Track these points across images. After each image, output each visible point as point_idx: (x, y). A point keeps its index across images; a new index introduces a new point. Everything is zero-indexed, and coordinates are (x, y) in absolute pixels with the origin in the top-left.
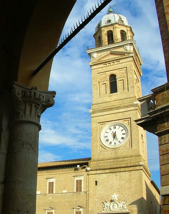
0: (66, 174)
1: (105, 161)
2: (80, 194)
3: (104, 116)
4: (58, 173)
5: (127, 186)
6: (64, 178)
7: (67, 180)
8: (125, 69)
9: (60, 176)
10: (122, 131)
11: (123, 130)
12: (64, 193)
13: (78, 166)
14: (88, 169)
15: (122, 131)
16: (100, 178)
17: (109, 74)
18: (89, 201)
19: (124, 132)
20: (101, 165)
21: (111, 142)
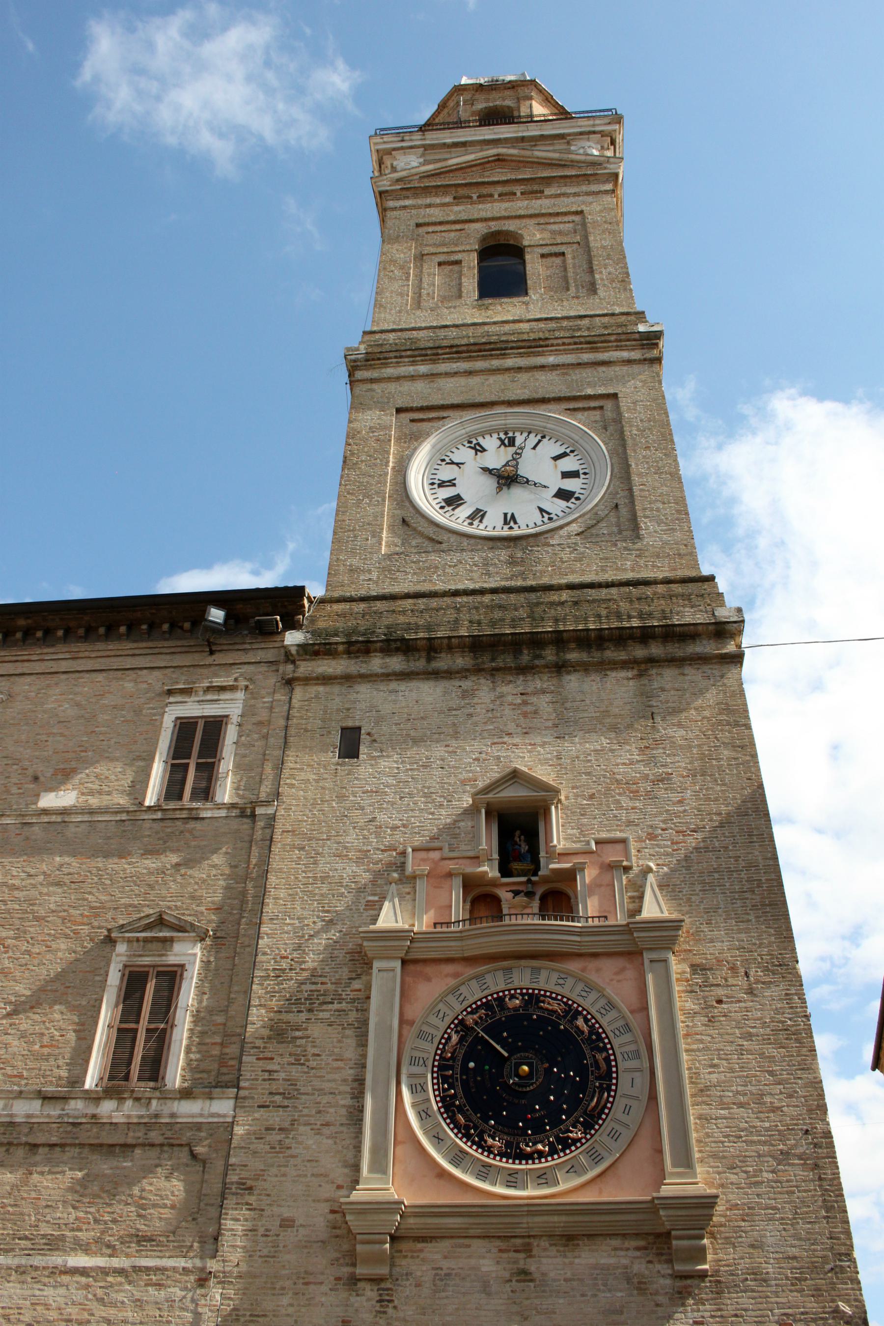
0: (100, 677)
1: (434, 603)
2: (192, 825)
3: (442, 382)
4: (39, 667)
5: (621, 769)
6: (78, 705)
7: (103, 717)
8: (577, 218)
9: (49, 686)
10: (556, 458)
11: (564, 455)
12: (45, 812)
13: (217, 615)
14: (293, 638)
15: (556, 458)
16: (386, 708)
17: (480, 229)
18: (272, 879)
19: (570, 464)
20: (402, 619)
21: (478, 511)
